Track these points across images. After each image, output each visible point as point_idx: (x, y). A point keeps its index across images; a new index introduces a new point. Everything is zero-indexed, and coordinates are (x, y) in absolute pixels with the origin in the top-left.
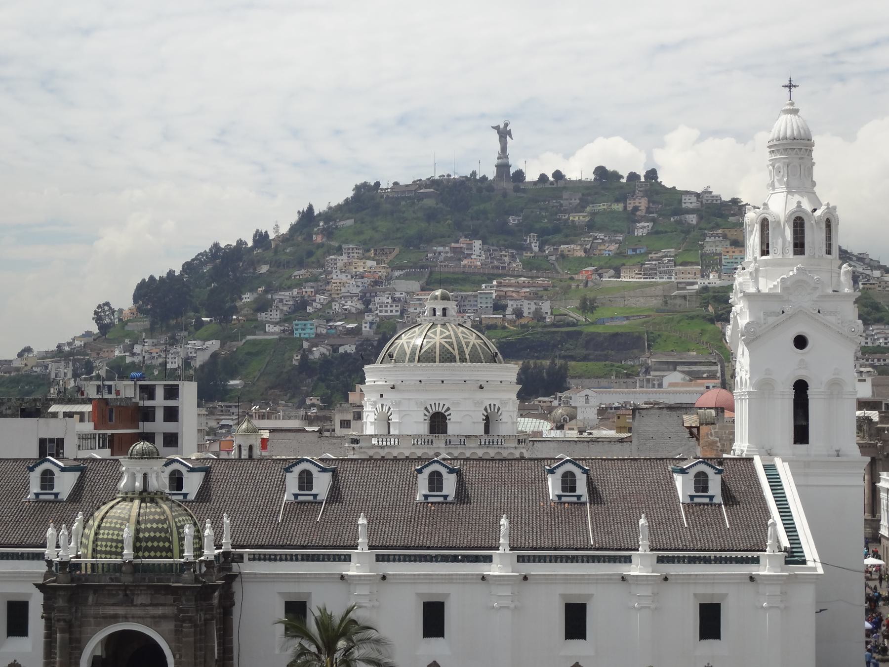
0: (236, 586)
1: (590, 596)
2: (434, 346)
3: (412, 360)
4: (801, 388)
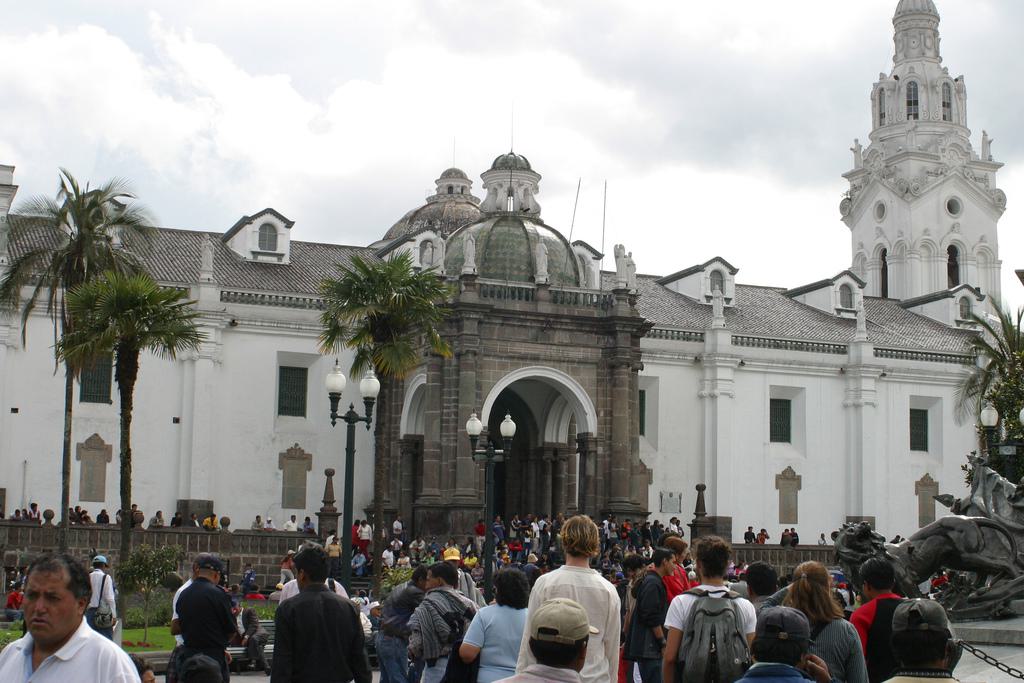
4: (953, 251)
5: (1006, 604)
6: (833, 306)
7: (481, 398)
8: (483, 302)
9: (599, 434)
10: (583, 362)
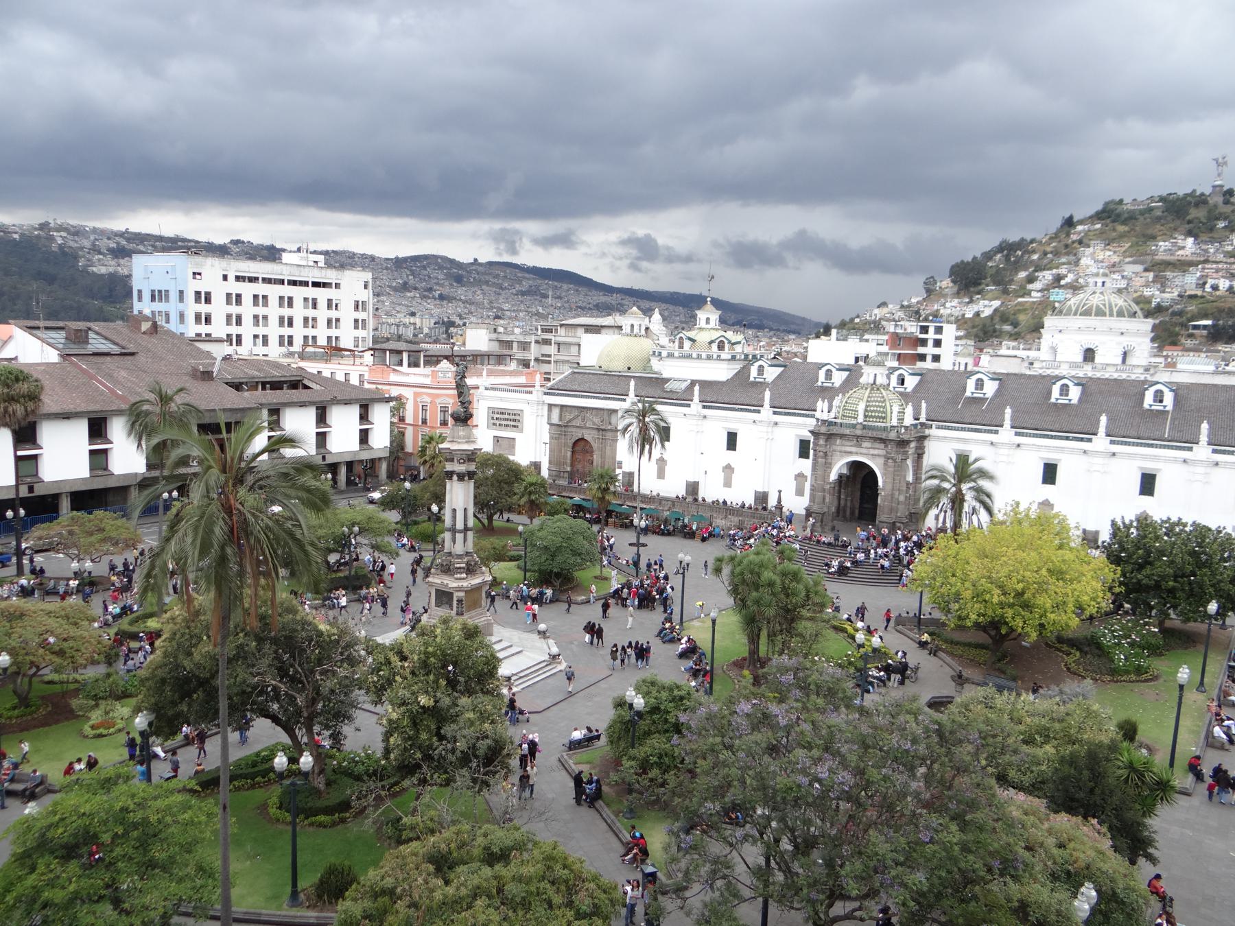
0: (926, 443)
1: (1159, 470)
2: (1092, 306)
3: (1075, 314)
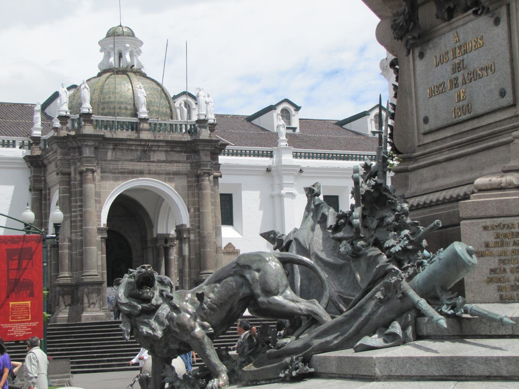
5: (307, 361)
6: (370, 130)
7: (100, 203)
8: (96, 133)
9: (192, 225)
10: (177, 174)
